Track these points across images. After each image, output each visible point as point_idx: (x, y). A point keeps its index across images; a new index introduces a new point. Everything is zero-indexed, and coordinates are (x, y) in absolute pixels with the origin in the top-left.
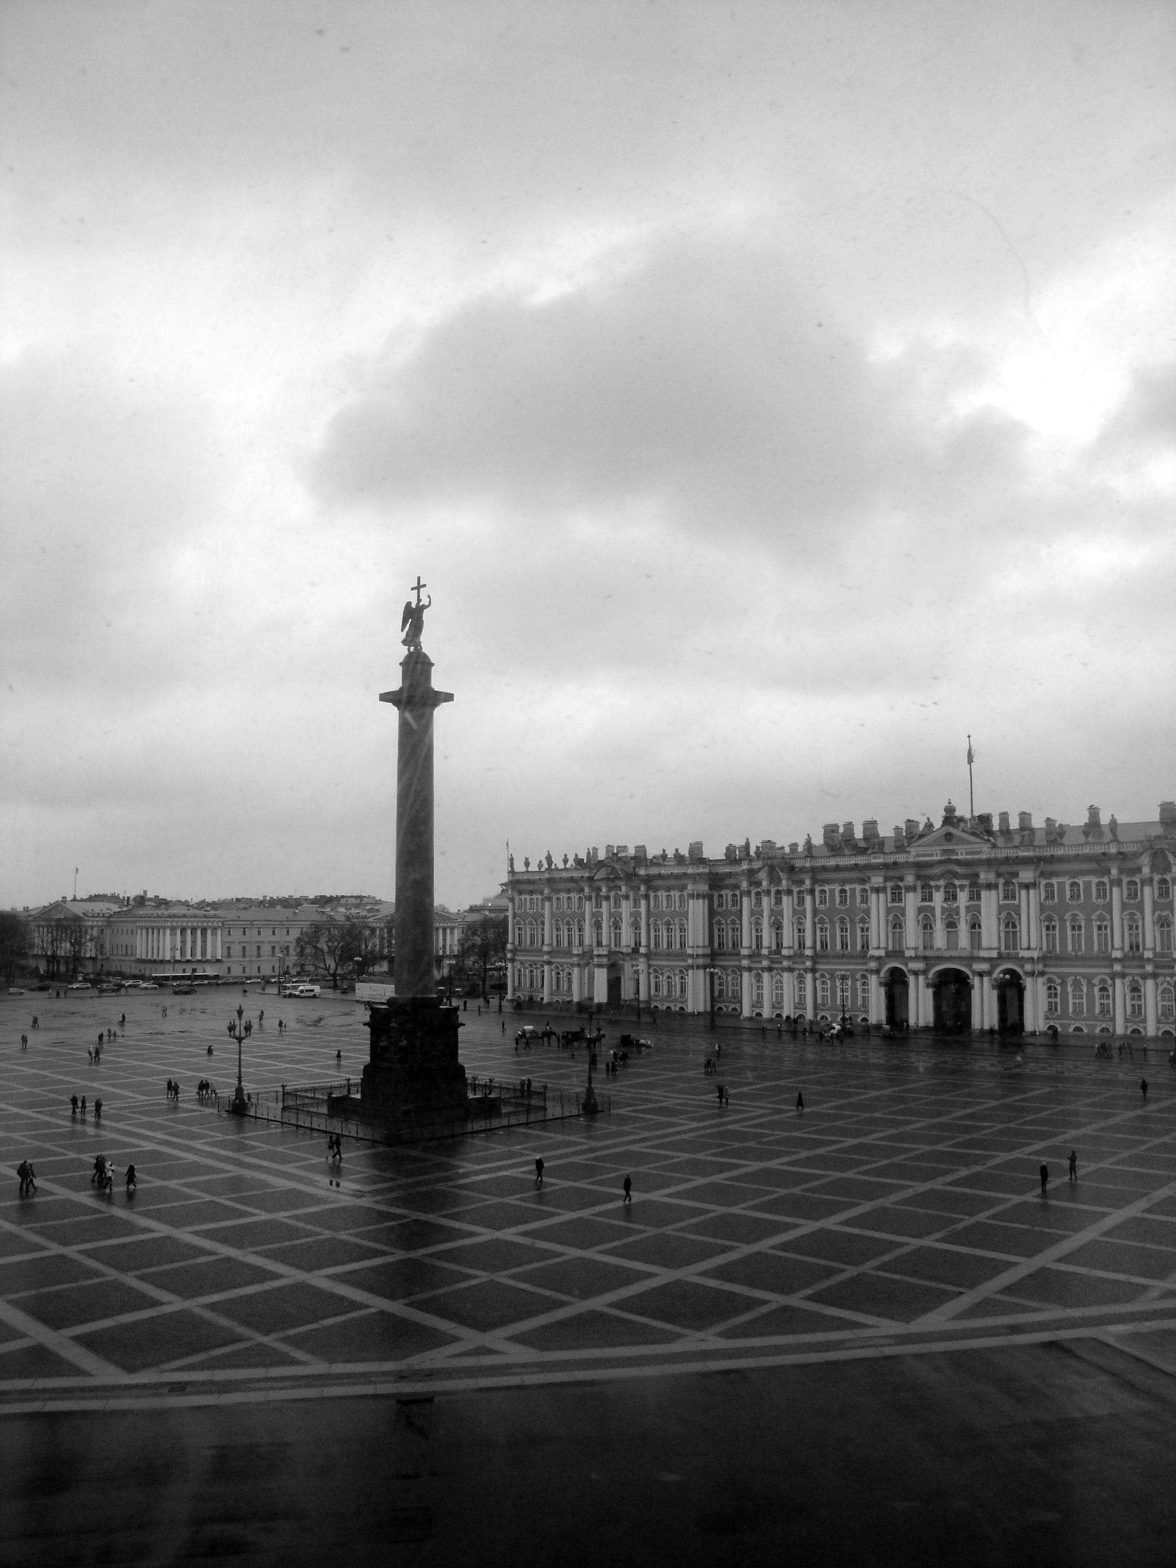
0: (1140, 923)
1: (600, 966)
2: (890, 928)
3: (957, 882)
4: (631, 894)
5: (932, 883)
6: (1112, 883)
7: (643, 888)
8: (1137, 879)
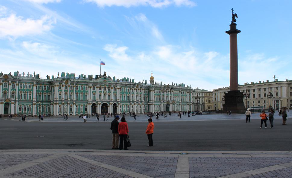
1: (13, 103)
3: (106, 87)
4: (12, 83)
5: (102, 87)
6: (130, 89)
7: (17, 82)
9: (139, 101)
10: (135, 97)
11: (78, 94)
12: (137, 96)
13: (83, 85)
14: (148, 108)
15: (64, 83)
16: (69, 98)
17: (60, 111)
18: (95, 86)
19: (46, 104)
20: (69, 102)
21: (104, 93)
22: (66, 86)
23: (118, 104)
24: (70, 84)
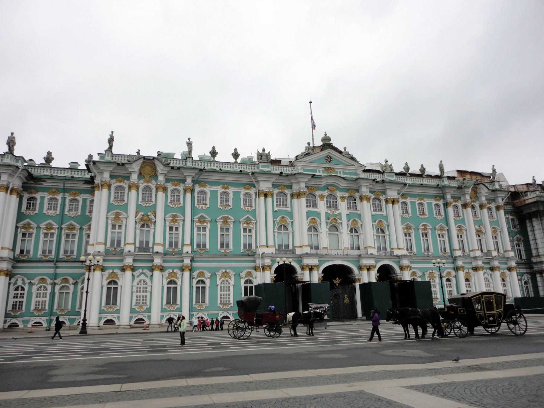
0: (465, 233)
2: (276, 230)
3: (338, 194)
5: (317, 193)
6: (446, 205)
8: (459, 204)
9: (495, 254)
10: (475, 238)
11: (208, 225)
12: (479, 233)
13: (226, 185)
14: (530, 285)
15: (134, 177)
16: (159, 239)
17: (115, 303)
18: (288, 192)
19: (69, 275)
20: (158, 261)
21: (328, 218)
22: (147, 188)
23: (402, 268)
24: (167, 180)
